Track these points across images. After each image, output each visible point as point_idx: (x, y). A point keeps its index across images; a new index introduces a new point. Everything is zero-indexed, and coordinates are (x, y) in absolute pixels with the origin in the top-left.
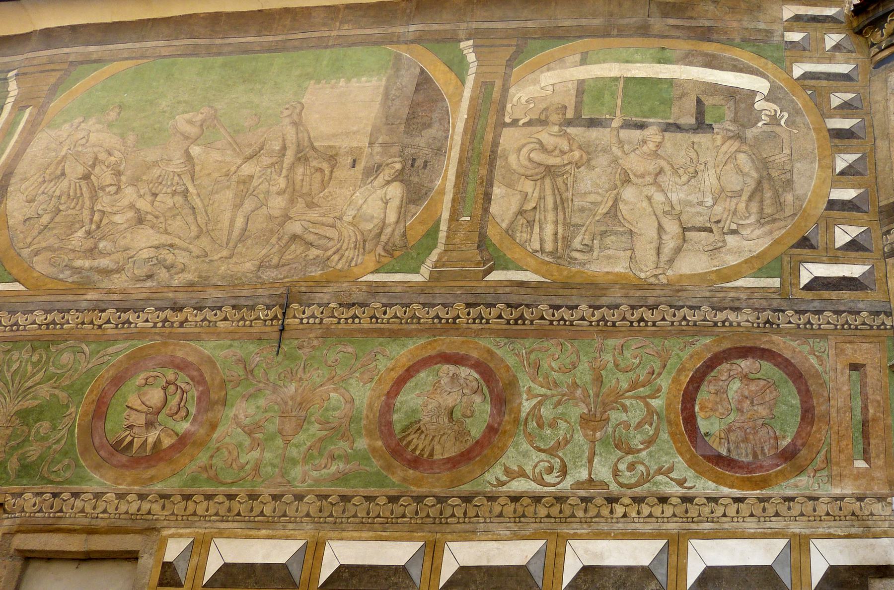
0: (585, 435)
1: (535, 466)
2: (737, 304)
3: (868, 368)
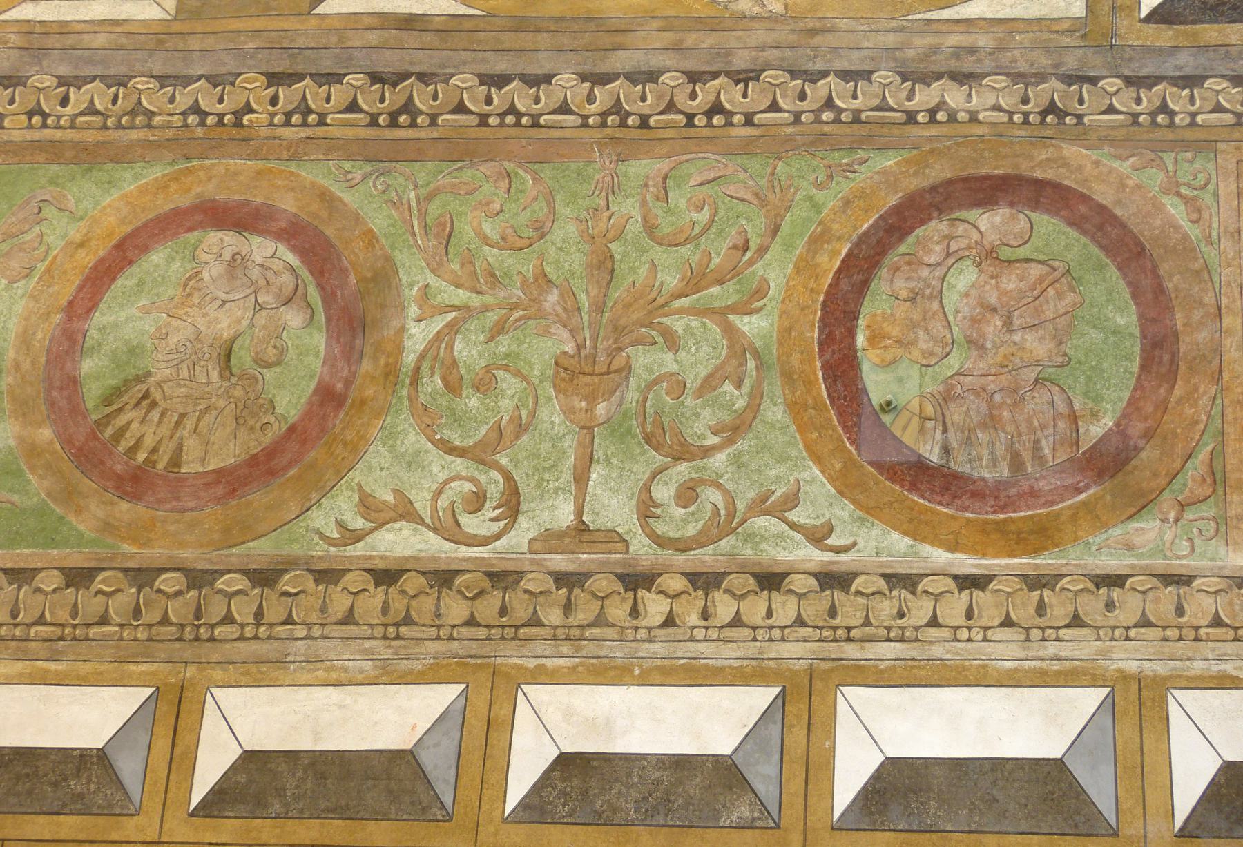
0: (568, 412)
1: (439, 493)
2: (968, 65)
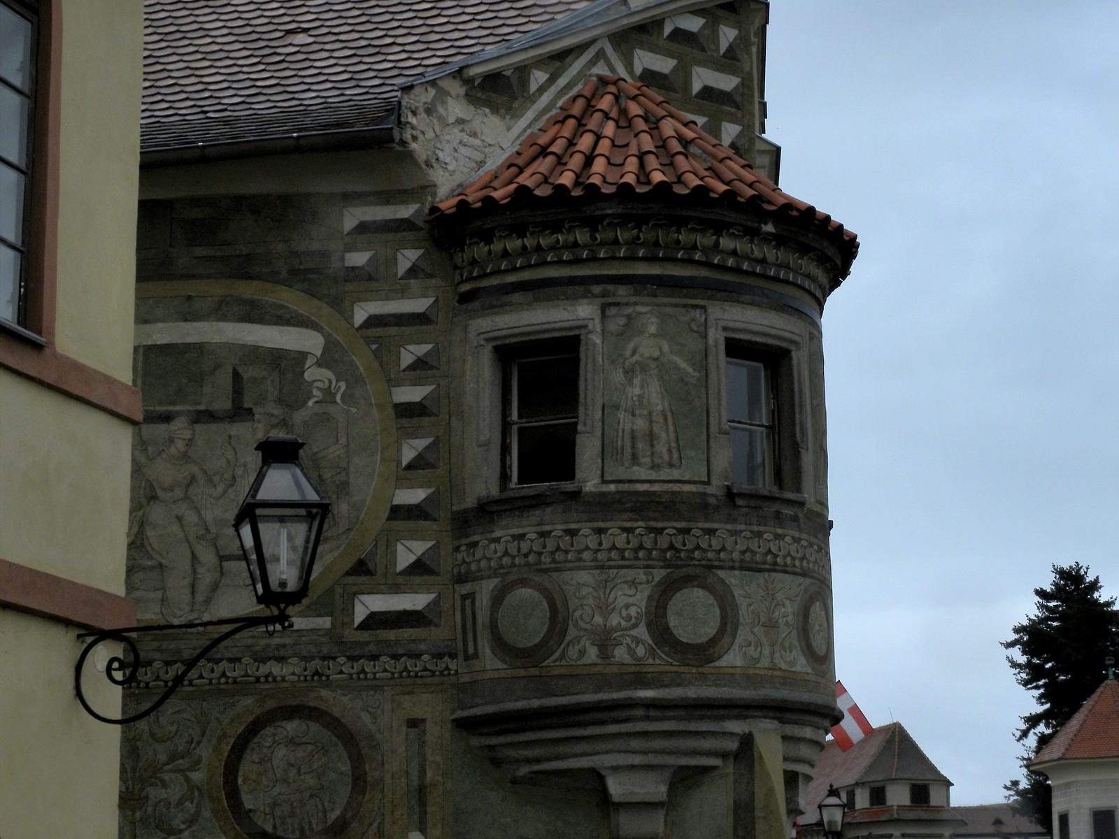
2: (282, 653)
3: (427, 722)
